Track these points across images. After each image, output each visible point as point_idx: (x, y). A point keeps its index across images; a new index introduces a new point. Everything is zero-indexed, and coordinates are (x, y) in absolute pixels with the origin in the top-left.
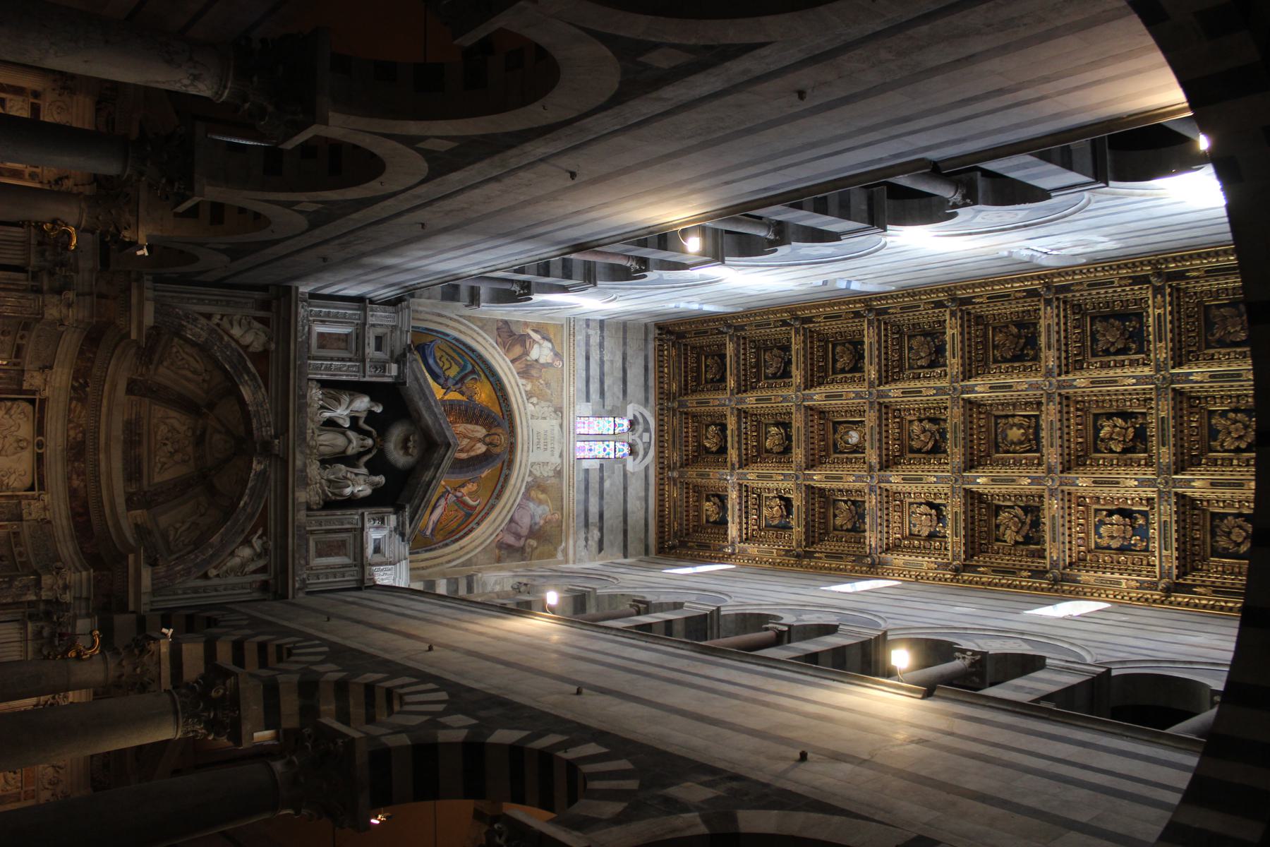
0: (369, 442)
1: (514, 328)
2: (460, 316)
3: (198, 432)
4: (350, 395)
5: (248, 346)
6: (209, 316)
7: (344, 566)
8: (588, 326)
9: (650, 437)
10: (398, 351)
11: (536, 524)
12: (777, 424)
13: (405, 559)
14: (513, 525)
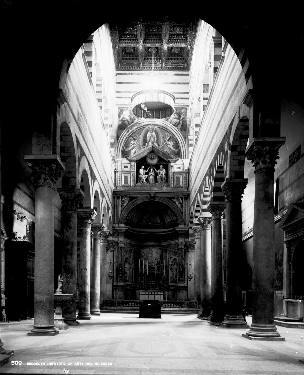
0: (152, 170)
4: (139, 175)
10: (128, 162)
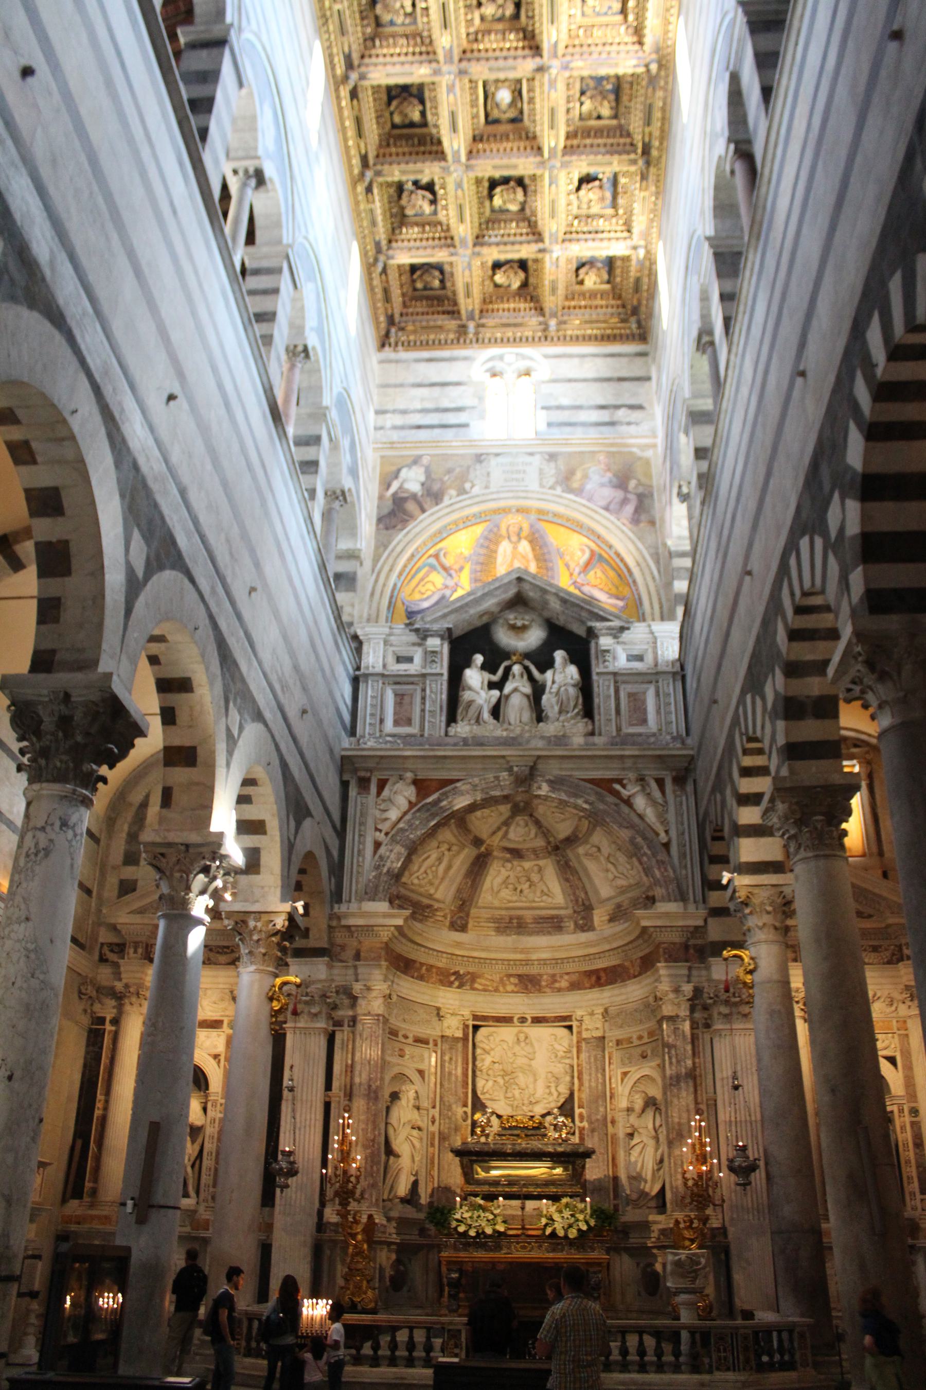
0: (516, 669)
1: (386, 511)
2: (373, 571)
3: (508, 856)
5: (410, 802)
6: (377, 845)
7: (657, 694)
8: (381, 428)
9: (509, 353)
10: (413, 638)
11: (610, 482)
12: (491, 197)
13: (649, 626)
14: (612, 507)
